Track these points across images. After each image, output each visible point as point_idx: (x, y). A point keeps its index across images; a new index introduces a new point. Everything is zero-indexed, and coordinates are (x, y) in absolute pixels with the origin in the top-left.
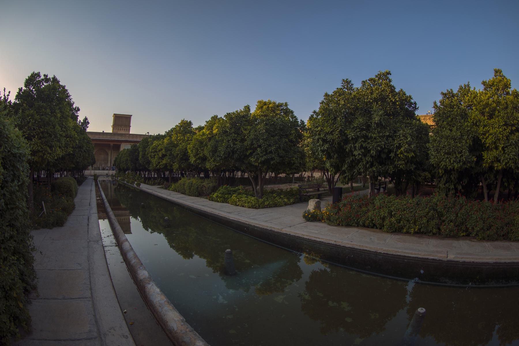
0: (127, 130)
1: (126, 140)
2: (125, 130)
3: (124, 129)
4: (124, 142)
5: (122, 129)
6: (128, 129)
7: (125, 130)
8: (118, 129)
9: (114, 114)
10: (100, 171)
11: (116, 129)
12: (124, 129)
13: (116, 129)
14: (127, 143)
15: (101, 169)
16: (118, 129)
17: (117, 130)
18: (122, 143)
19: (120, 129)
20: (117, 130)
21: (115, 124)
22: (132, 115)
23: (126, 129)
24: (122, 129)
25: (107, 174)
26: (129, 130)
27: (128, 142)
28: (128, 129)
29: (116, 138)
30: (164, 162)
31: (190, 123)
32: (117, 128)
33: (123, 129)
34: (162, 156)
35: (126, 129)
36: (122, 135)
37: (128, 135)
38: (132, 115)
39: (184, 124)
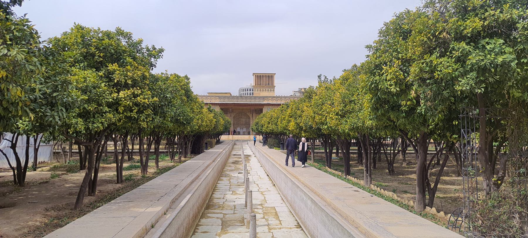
0: (271, 90)
2: (268, 90)
4: (266, 105)
7: (268, 90)
8: (260, 90)
11: (258, 90)
12: (267, 89)
13: (258, 90)
14: (271, 107)
15: (241, 133)
16: (260, 90)
17: (259, 91)
19: (263, 90)
20: (259, 91)
21: (256, 85)
24: (264, 89)
26: (274, 90)
32: (259, 89)
33: (266, 90)
36: (264, 98)
37: (271, 98)
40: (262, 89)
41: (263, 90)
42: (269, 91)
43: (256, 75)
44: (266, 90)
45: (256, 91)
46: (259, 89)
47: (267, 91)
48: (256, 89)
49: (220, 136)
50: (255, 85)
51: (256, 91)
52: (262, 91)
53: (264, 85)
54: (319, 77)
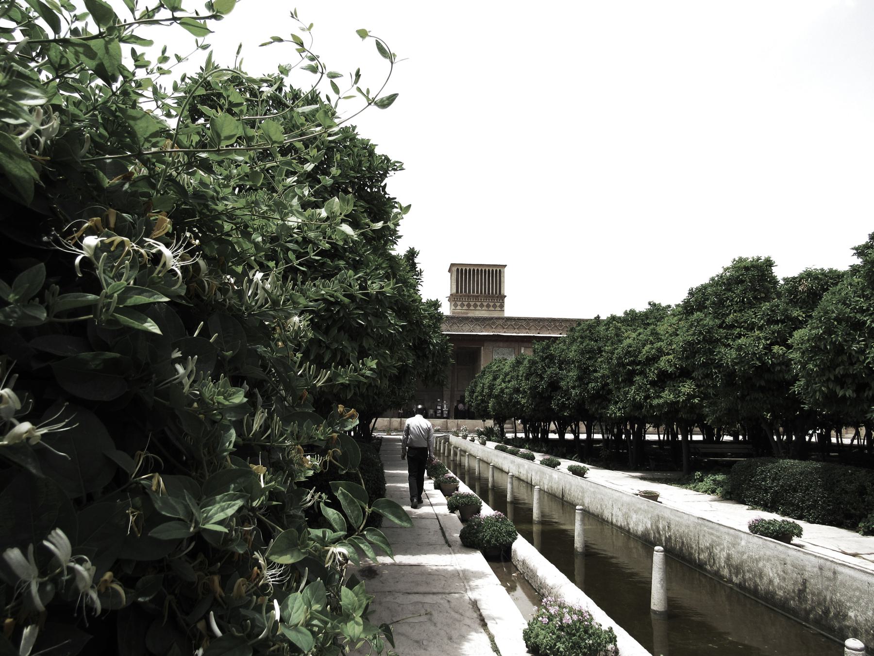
0: (495, 306)
2: (488, 306)
3: (485, 304)
4: (490, 340)
5: (479, 304)
7: (488, 306)
8: (469, 306)
9: (452, 265)
13: (462, 305)
16: (469, 306)
17: (465, 308)
19: (475, 306)
20: (465, 308)
24: (479, 304)
27: (501, 341)
28: (498, 304)
29: (466, 331)
30: (667, 396)
31: (769, 263)
32: (466, 303)
33: (482, 306)
34: (658, 376)
35: (492, 304)
37: (501, 322)
39: (747, 269)
40: (472, 304)
41: (475, 306)
42: (491, 308)
44: (482, 306)
45: (459, 307)
46: (466, 303)
48: (459, 303)
49: (373, 421)
50: (454, 291)
51: (459, 307)
52: (472, 308)
53: (477, 292)
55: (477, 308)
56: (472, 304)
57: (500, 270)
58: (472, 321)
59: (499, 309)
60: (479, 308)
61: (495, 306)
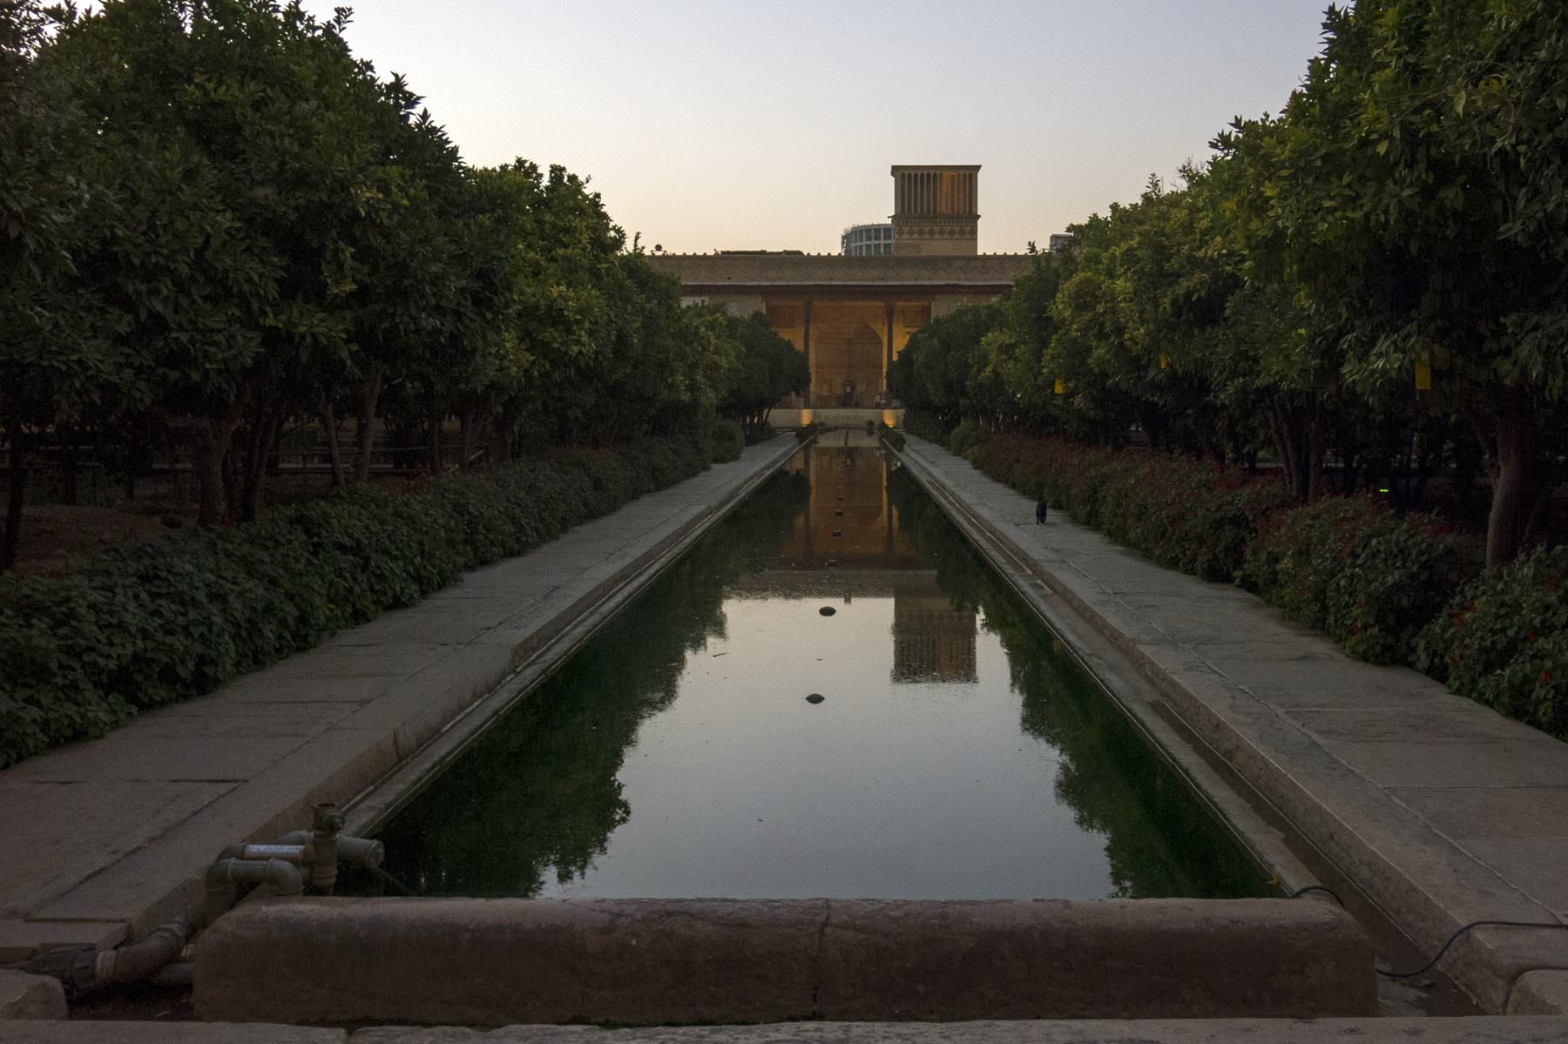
0: (962, 233)
1: (954, 285)
6: (967, 229)
7: (952, 233)
10: (843, 412)
11: (911, 233)
13: (911, 233)
16: (921, 233)
17: (915, 236)
18: (938, 297)
19: (932, 233)
20: (915, 236)
22: (978, 168)
23: (957, 229)
24: (936, 229)
25: (871, 423)
26: (974, 232)
28: (967, 229)
32: (917, 229)
35: (957, 229)
36: (932, 263)
37: (960, 263)
38: (978, 168)
40: (926, 229)
41: (932, 233)
43: (903, 174)
44: (942, 232)
46: (917, 229)
47: (946, 236)
48: (906, 229)
49: (766, 411)
50: (899, 212)
54: (1153, 175)
55: (934, 237)
56: (926, 229)
57: (970, 174)
58: (916, 264)
59: (969, 237)
60: (936, 236)
61: (962, 233)
